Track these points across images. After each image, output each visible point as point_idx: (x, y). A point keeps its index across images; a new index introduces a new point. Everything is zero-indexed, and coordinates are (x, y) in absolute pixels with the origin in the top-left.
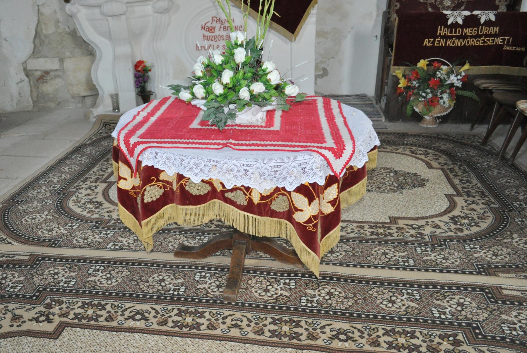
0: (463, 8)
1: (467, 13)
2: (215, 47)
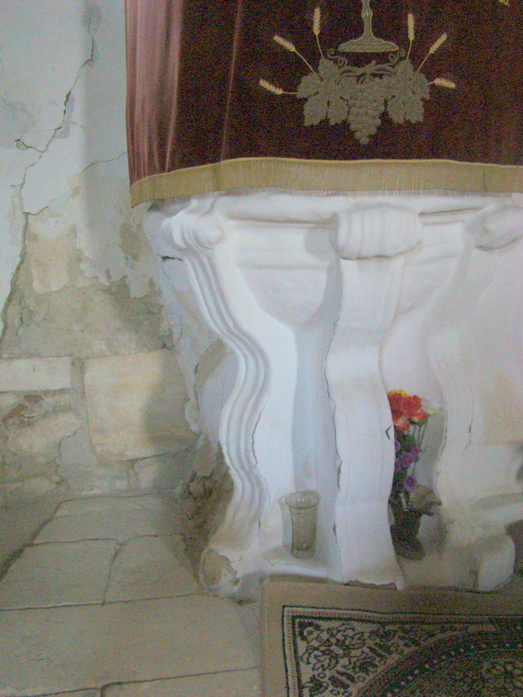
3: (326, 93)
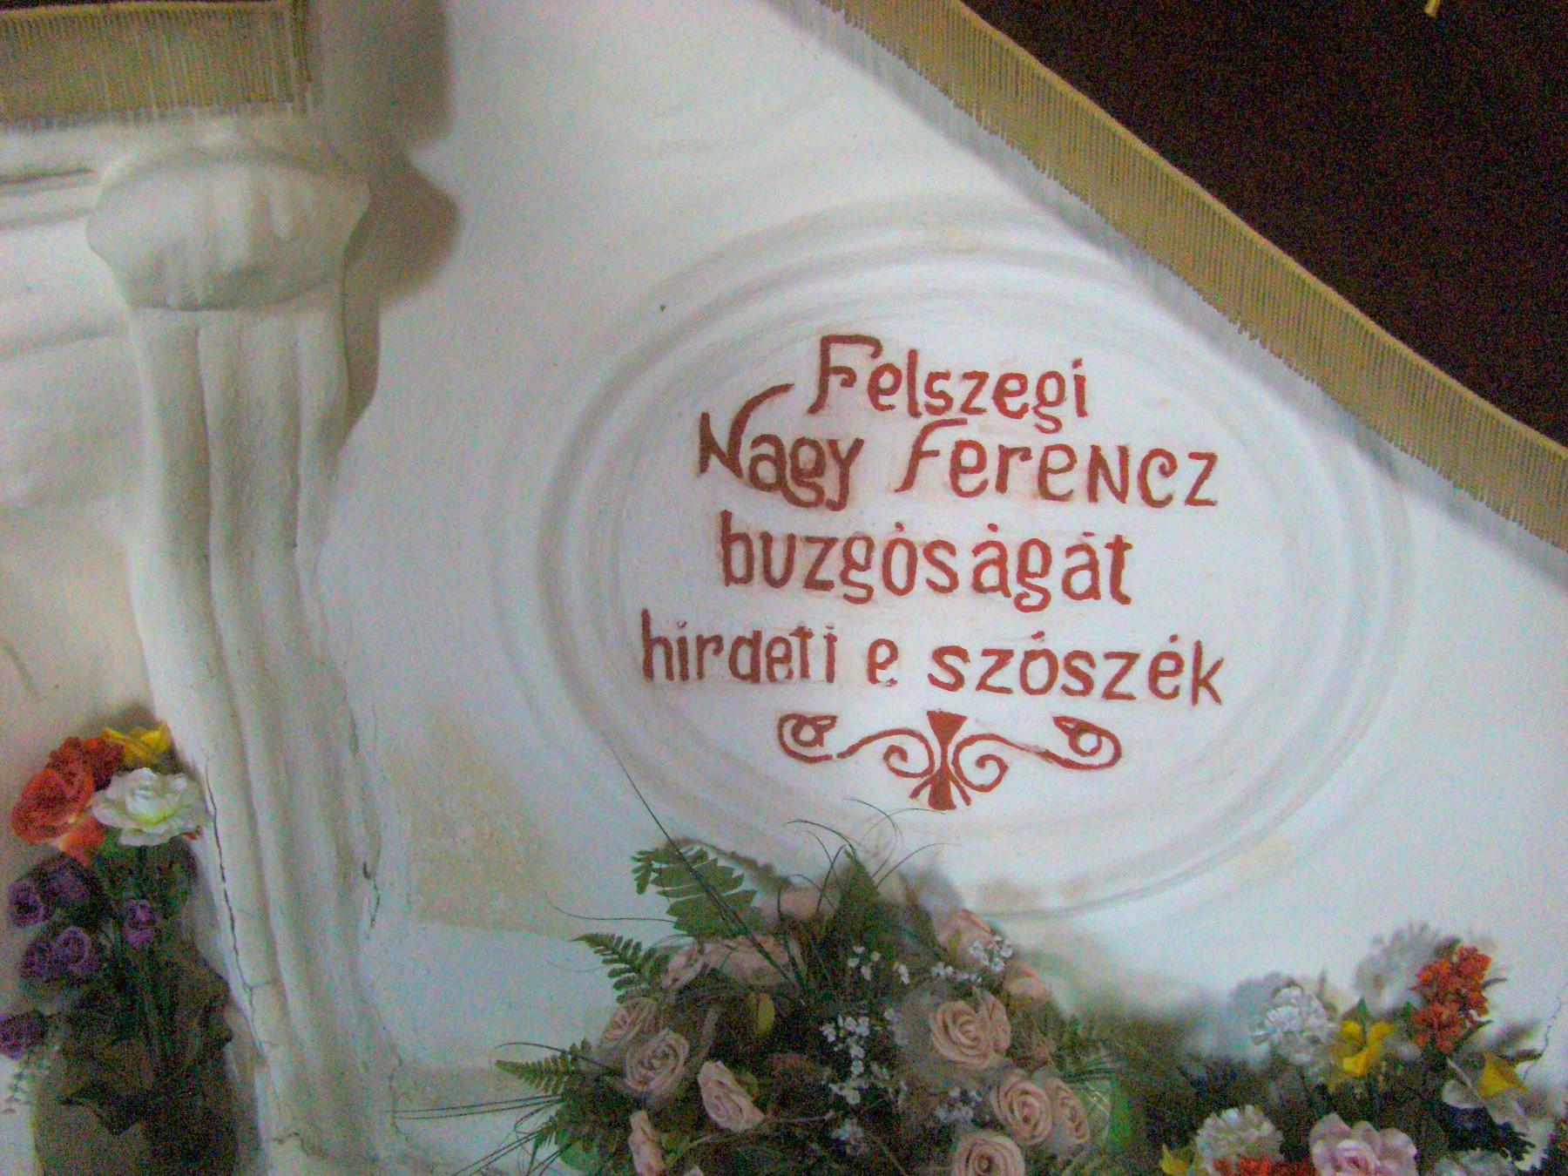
2: (852, 662)
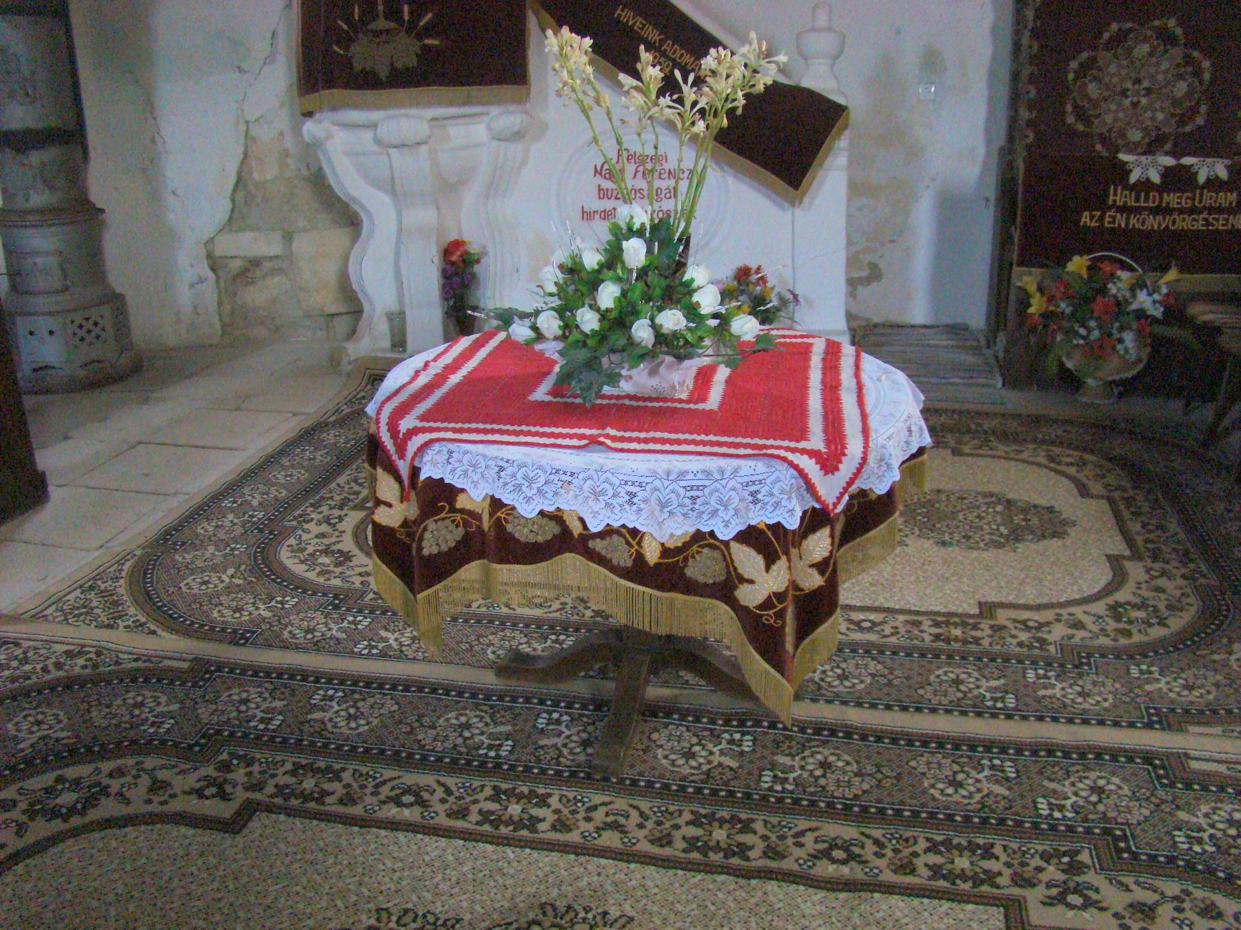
0: (1168, 147)
1: (1169, 161)
3: (362, 54)
